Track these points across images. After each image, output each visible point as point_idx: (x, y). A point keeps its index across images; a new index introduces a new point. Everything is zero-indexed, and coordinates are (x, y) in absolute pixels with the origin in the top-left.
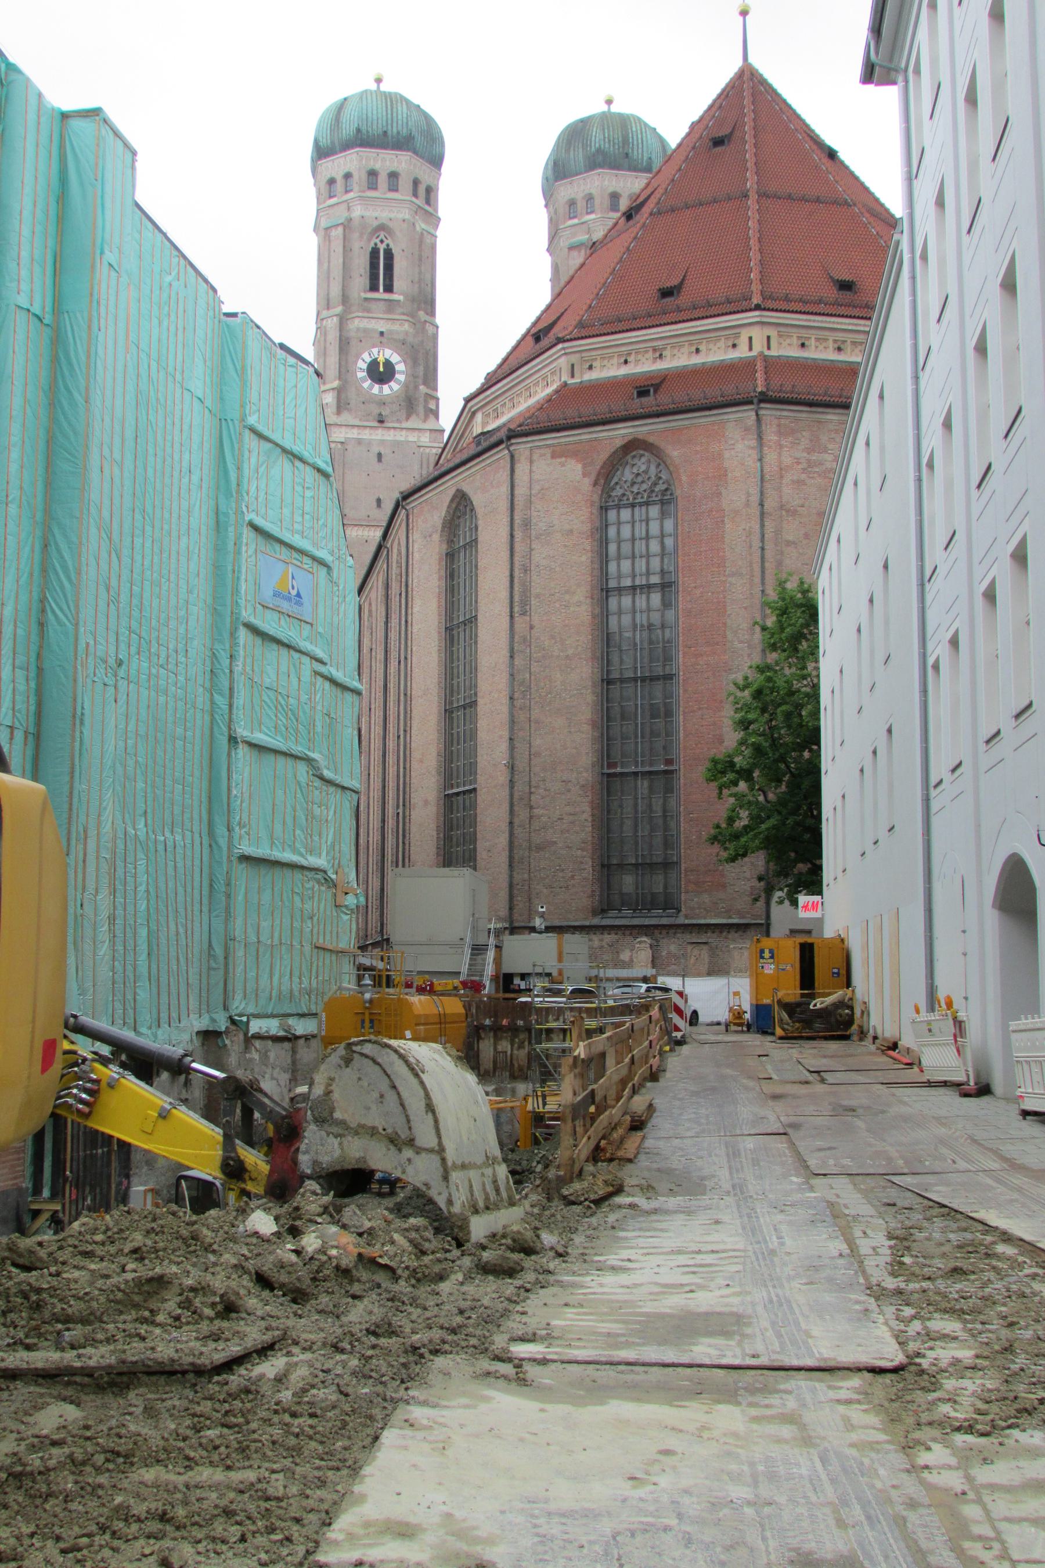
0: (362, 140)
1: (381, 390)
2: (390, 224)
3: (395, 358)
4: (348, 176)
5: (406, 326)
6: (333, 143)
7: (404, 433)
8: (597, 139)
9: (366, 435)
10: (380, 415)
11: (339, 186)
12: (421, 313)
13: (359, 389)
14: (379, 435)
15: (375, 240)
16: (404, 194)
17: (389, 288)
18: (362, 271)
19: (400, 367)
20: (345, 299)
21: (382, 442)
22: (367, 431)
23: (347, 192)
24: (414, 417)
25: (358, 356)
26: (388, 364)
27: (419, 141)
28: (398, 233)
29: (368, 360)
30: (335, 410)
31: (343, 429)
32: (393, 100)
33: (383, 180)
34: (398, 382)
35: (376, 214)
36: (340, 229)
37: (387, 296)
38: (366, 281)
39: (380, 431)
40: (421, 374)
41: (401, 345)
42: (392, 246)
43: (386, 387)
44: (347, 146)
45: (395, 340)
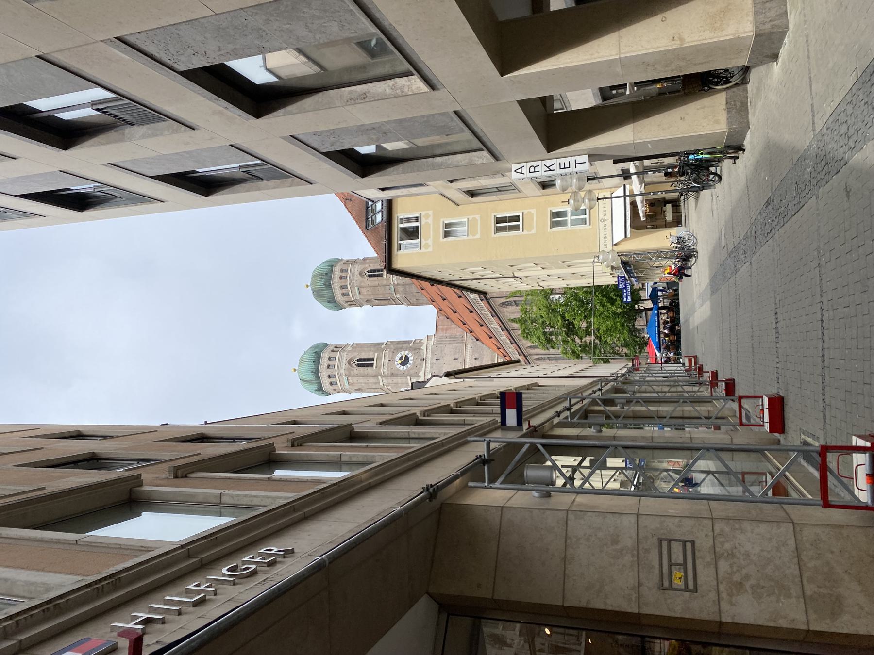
0: (316, 372)
1: (411, 360)
3: (399, 355)
4: (329, 377)
5: (387, 352)
6: (316, 383)
7: (428, 351)
8: (320, 285)
9: (429, 365)
11: (332, 380)
14: (429, 361)
15: (354, 366)
16: (337, 355)
17: (372, 360)
20: (376, 376)
22: (427, 365)
25: (398, 370)
26: (401, 358)
38: (369, 369)
39: (427, 360)
44: (318, 377)
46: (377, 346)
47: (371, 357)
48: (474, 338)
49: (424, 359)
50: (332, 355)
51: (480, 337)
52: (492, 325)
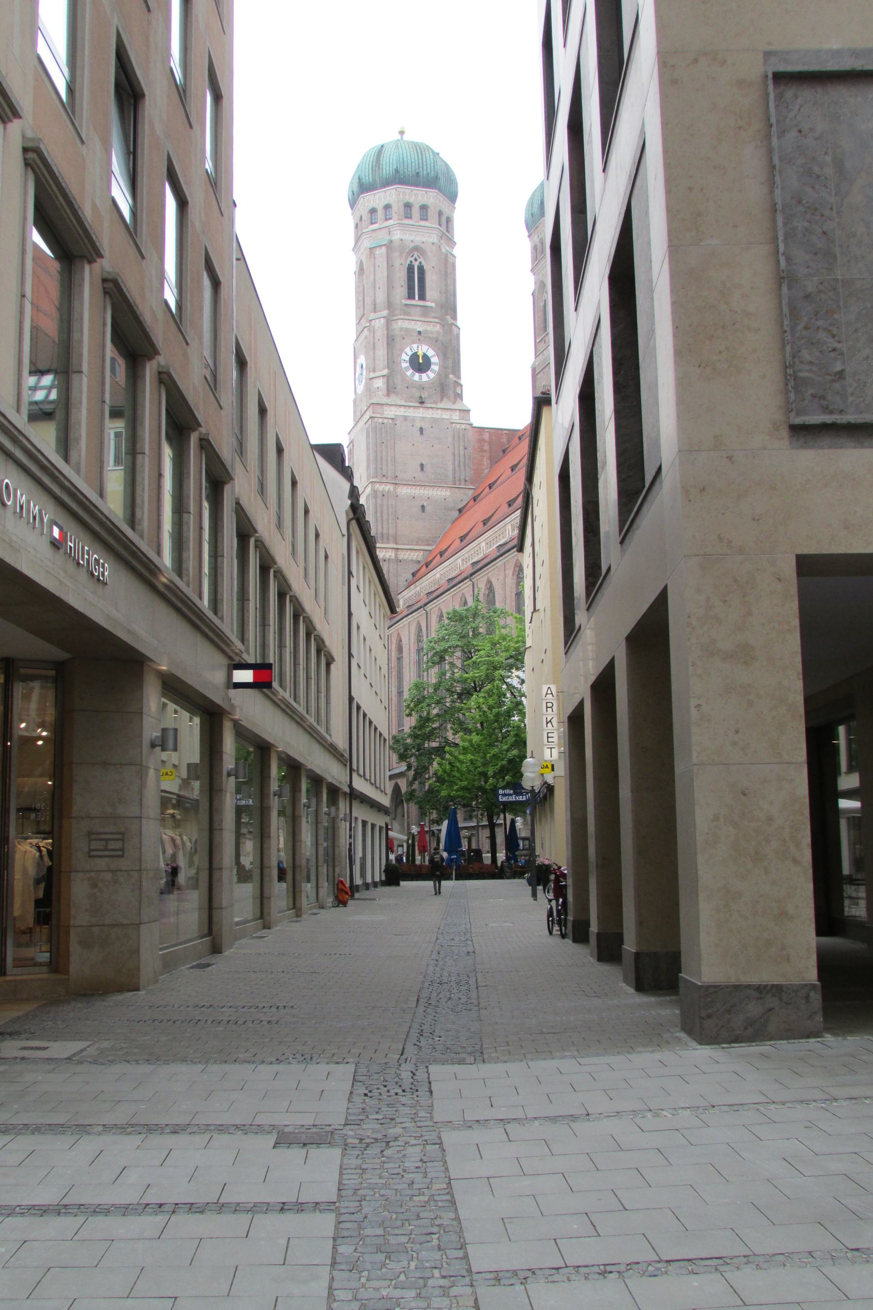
0: (399, 178)
1: (421, 378)
2: (423, 246)
3: (431, 353)
4: (387, 207)
5: (438, 326)
7: (439, 411)
9: (410, 413)
10: (421, 397)
11: (380, 214)
12: (448, 317)
13: (403, 376)
14: (420, 413)
15: (410, 259)
16: (432, 223)
17: (422, 297)
18: (403, 283)
19: (435, 360)
20: (390, 305)
21: (423, 419)
22: (411, 410)
23: (386, 220)
24: (445, 399)
25: (402, 350)
26: (425, 356)
27: (442, 181)
28: (429, 254)
29: (410, 353)
30: (385, 393)
31: (393, 408)
32: (421, 149)
33: (416, 211)
34: (433, 371)
35: (412, 238)
36: (384, 249)
37: (421, 303)
39: (421, 410)
40: (450, 365)
41: (434, 342)
42: (423, 263)
43: (424, 375)
44: (387, 183)
45: (430, 338)
46: (449, 307)
47: (429, 294)
48: (464, 503)
49: (422, 403)
50: (432, 214)
51: (465, 517)
52: (483, 544)
